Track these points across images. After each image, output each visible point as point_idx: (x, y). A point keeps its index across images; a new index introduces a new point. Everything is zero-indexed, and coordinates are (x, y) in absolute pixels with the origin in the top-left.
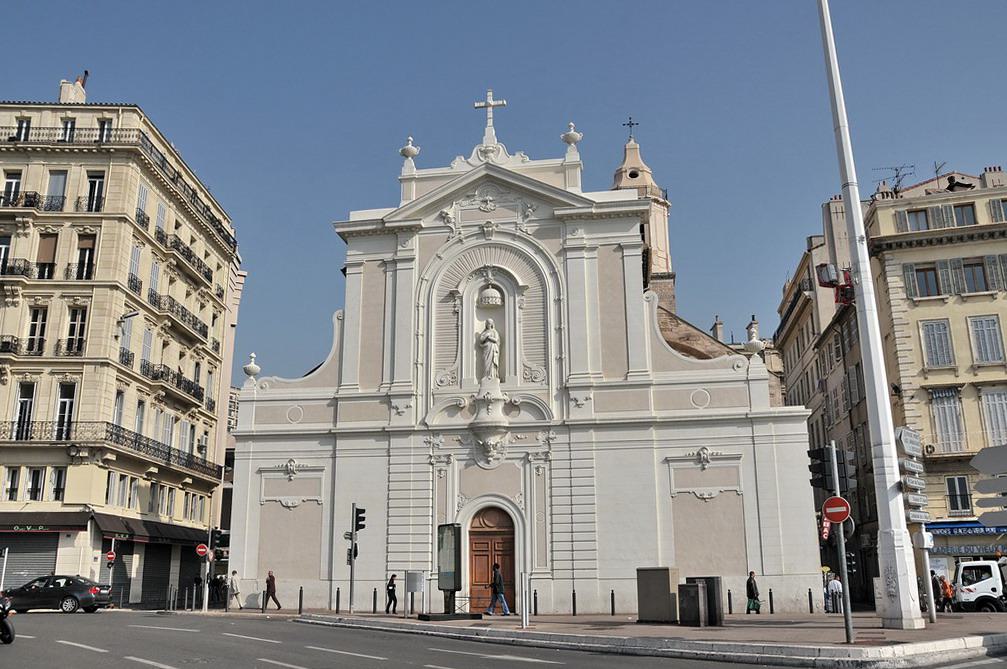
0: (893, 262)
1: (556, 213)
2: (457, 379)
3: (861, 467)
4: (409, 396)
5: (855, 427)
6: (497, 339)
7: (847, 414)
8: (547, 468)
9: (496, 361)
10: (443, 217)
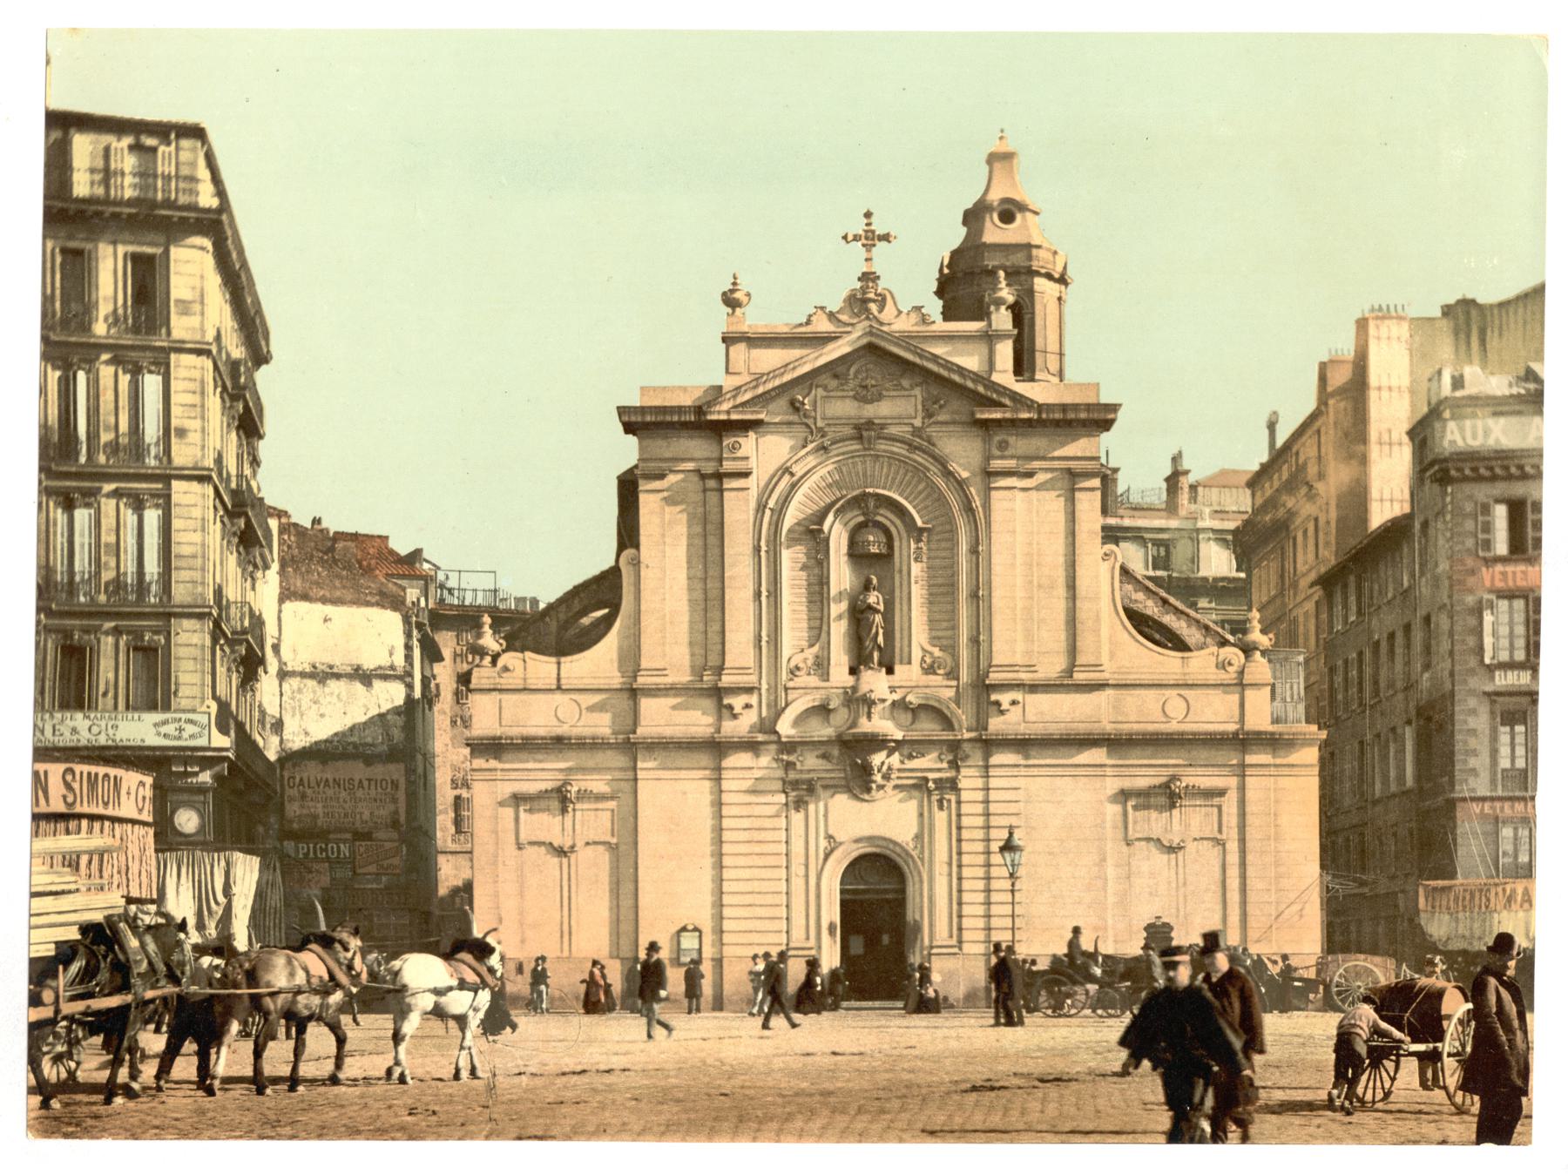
1: (979, 416)
2: (822, 666)
4: (749, 690)
6: (881, 607)
8: (953, 798)
9: (880, 639)
10: (795, 407)
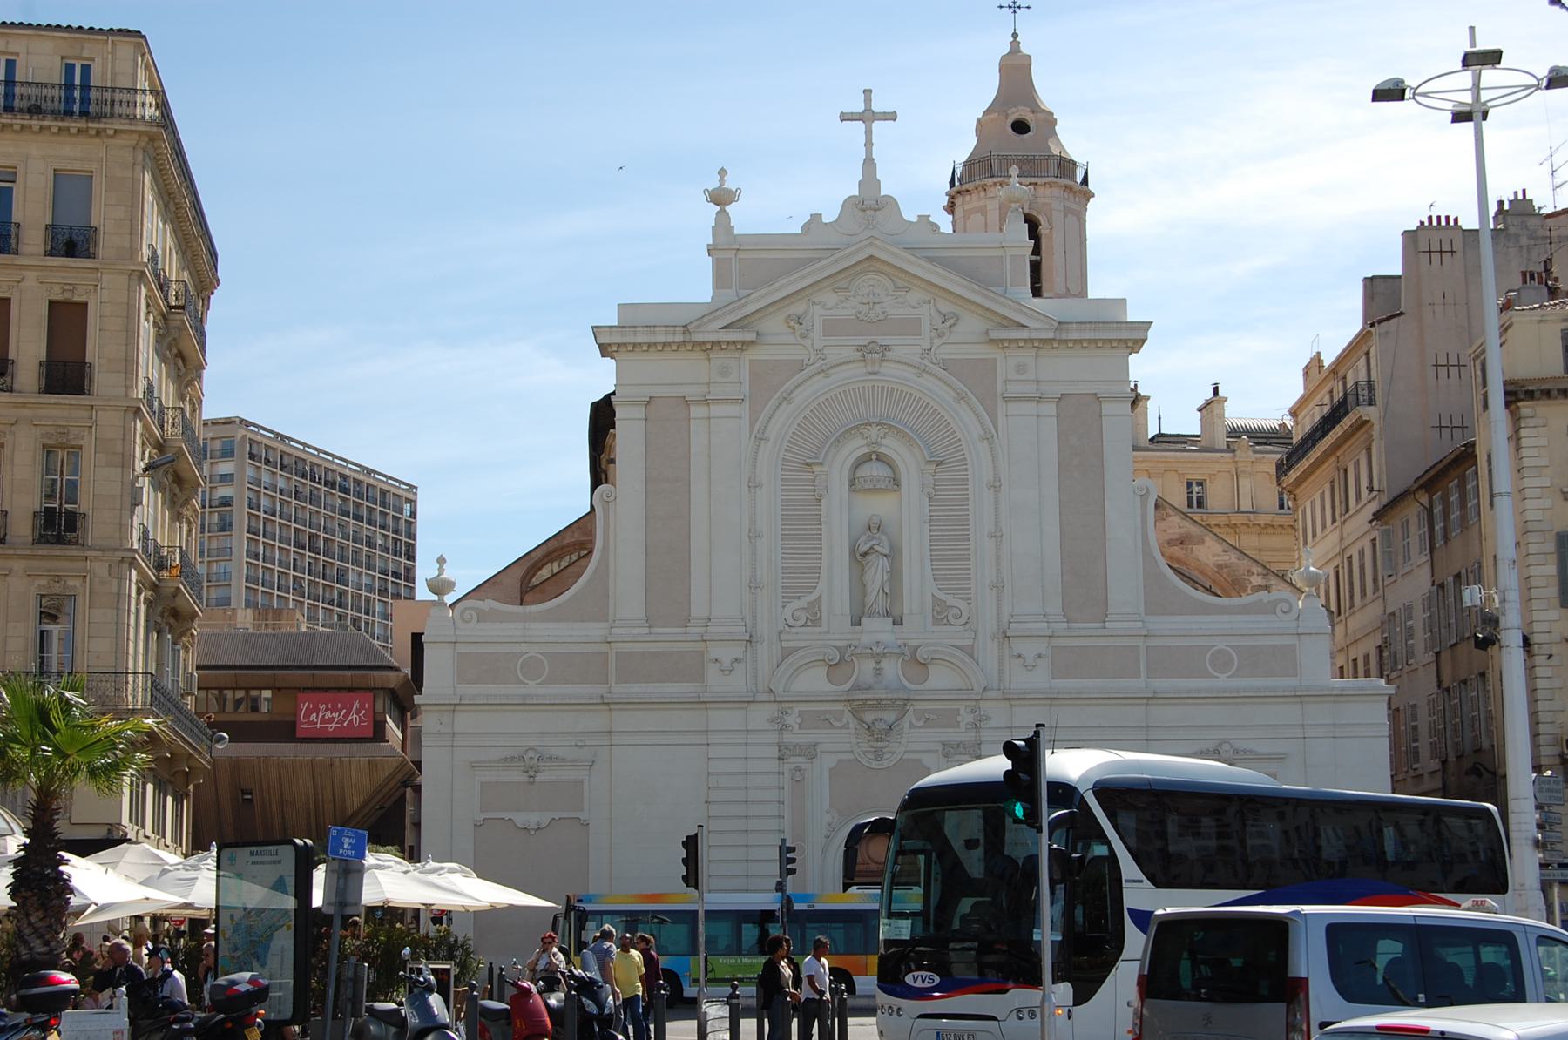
0: (1532, 422)
3: (1452, 758)
5: (1445, 685)
7: (1430, 657)
